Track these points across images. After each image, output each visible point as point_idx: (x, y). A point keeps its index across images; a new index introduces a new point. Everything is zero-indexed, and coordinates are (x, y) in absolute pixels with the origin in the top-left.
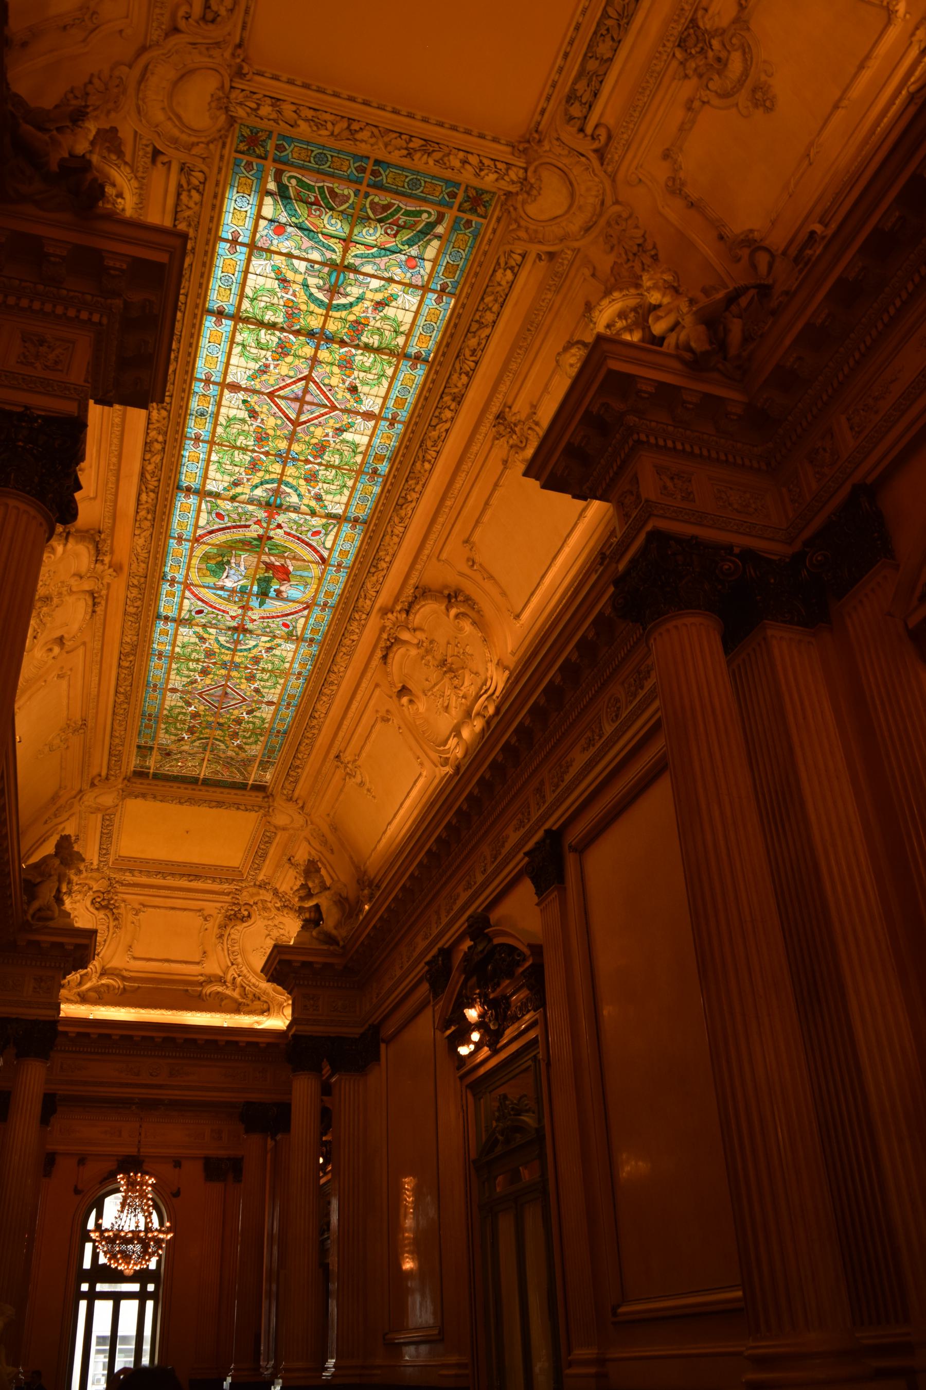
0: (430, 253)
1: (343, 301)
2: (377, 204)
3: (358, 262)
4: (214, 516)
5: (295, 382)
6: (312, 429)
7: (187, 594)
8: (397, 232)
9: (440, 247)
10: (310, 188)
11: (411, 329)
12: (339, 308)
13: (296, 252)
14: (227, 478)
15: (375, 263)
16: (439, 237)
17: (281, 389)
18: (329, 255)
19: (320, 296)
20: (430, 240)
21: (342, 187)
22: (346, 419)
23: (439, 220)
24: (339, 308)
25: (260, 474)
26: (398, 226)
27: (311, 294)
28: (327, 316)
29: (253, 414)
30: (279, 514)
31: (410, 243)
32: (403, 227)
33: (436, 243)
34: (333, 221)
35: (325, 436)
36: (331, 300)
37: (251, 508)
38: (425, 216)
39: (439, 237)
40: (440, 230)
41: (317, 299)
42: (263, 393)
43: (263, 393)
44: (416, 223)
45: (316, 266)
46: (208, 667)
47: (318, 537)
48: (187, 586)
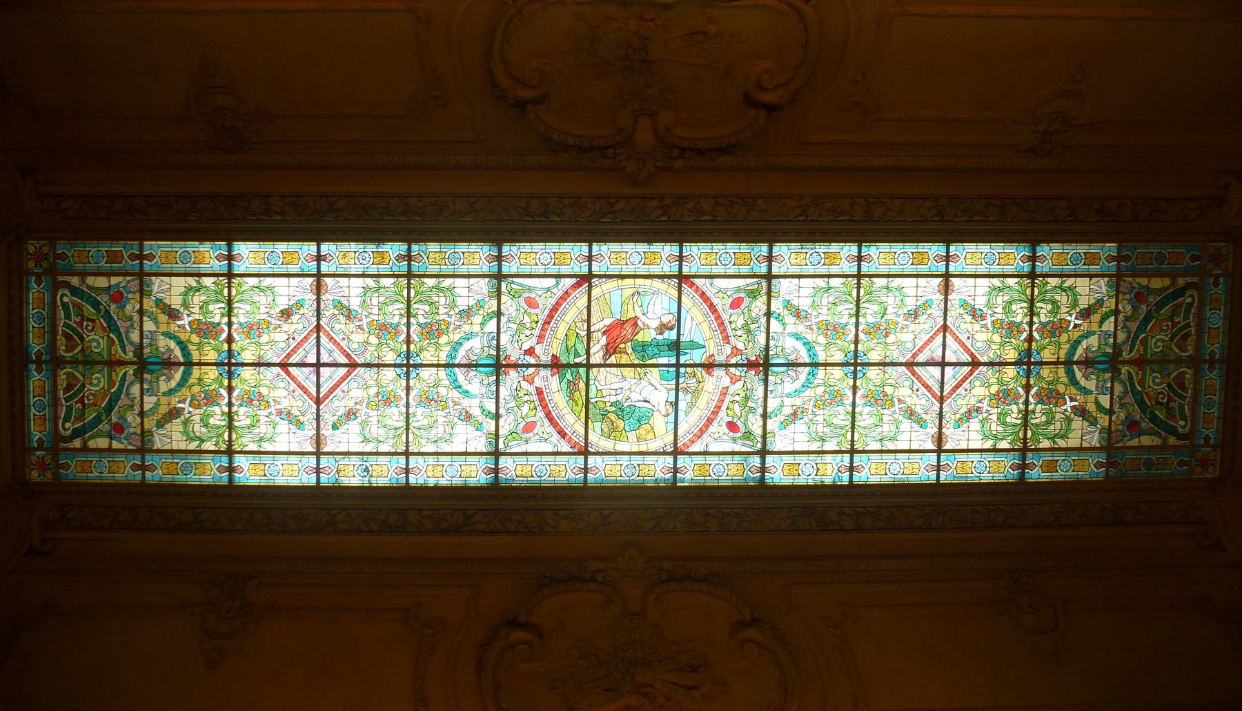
0: (1146, 440)
1: (1078, 374)
2: (1184, 378)
3: (1124, 377)
4: (735, 296)
5: (967, 350)
6: (907, 383)
7: (570, 282)
8: (1162, 404)
9: (1156, 447)
10: (1186, 317)
11: (1060, 449)
12: (1071, 374)
13: (1121, 317)
14: (809, 301)
15: (1126, 393)
16: (1165, 440)
17: (957, 339)
18: (1127, 347)
19: (1080, 351)
20: (1159, 436)
21: (1194, 343)
22: (931, 418)
23: (1180, 437)
24: (1071, 374)
25: (822, 339)
26: (1168, 401)
27: (1080, 343)
28: (1057, 363)
29: (915, 314)
30: (757, 374)
31: (1154, 419)
32: (1168, 408)
33: (1157, 441)
34: (1160, 344)
35: (900, 401)
36: (1077, 363)
37: (762, 339)
38: (1182, 423)
39: (1165, 440)
40: (1172, 441)
41: (1075, 349)
42: (945, 319)
43: (945, 319)
44: (1174, 418)
45: (1111, 340)
46: (397, 333)
47: (727, 431)
48: (586, 279)
